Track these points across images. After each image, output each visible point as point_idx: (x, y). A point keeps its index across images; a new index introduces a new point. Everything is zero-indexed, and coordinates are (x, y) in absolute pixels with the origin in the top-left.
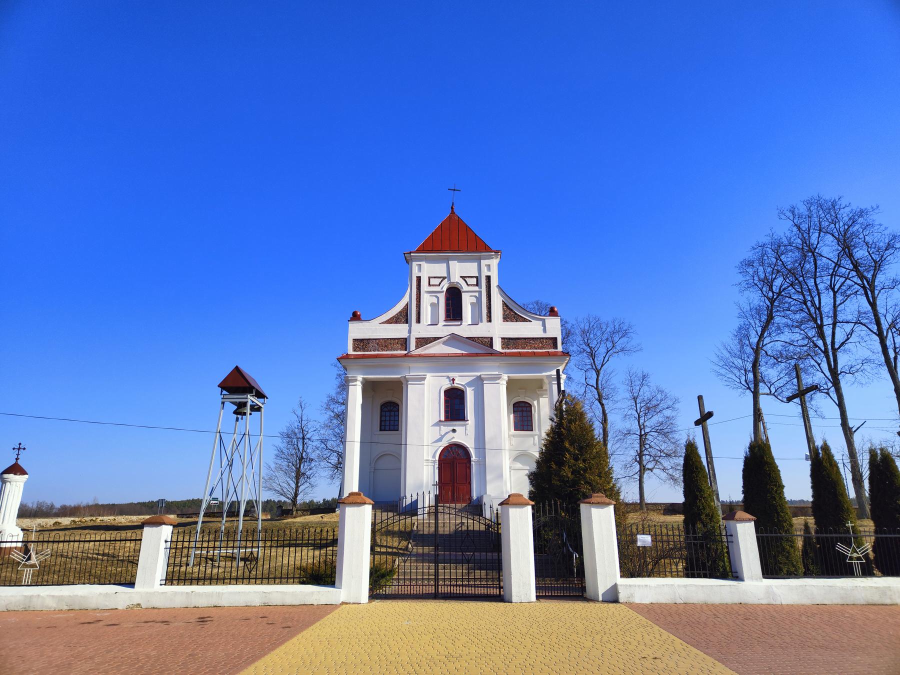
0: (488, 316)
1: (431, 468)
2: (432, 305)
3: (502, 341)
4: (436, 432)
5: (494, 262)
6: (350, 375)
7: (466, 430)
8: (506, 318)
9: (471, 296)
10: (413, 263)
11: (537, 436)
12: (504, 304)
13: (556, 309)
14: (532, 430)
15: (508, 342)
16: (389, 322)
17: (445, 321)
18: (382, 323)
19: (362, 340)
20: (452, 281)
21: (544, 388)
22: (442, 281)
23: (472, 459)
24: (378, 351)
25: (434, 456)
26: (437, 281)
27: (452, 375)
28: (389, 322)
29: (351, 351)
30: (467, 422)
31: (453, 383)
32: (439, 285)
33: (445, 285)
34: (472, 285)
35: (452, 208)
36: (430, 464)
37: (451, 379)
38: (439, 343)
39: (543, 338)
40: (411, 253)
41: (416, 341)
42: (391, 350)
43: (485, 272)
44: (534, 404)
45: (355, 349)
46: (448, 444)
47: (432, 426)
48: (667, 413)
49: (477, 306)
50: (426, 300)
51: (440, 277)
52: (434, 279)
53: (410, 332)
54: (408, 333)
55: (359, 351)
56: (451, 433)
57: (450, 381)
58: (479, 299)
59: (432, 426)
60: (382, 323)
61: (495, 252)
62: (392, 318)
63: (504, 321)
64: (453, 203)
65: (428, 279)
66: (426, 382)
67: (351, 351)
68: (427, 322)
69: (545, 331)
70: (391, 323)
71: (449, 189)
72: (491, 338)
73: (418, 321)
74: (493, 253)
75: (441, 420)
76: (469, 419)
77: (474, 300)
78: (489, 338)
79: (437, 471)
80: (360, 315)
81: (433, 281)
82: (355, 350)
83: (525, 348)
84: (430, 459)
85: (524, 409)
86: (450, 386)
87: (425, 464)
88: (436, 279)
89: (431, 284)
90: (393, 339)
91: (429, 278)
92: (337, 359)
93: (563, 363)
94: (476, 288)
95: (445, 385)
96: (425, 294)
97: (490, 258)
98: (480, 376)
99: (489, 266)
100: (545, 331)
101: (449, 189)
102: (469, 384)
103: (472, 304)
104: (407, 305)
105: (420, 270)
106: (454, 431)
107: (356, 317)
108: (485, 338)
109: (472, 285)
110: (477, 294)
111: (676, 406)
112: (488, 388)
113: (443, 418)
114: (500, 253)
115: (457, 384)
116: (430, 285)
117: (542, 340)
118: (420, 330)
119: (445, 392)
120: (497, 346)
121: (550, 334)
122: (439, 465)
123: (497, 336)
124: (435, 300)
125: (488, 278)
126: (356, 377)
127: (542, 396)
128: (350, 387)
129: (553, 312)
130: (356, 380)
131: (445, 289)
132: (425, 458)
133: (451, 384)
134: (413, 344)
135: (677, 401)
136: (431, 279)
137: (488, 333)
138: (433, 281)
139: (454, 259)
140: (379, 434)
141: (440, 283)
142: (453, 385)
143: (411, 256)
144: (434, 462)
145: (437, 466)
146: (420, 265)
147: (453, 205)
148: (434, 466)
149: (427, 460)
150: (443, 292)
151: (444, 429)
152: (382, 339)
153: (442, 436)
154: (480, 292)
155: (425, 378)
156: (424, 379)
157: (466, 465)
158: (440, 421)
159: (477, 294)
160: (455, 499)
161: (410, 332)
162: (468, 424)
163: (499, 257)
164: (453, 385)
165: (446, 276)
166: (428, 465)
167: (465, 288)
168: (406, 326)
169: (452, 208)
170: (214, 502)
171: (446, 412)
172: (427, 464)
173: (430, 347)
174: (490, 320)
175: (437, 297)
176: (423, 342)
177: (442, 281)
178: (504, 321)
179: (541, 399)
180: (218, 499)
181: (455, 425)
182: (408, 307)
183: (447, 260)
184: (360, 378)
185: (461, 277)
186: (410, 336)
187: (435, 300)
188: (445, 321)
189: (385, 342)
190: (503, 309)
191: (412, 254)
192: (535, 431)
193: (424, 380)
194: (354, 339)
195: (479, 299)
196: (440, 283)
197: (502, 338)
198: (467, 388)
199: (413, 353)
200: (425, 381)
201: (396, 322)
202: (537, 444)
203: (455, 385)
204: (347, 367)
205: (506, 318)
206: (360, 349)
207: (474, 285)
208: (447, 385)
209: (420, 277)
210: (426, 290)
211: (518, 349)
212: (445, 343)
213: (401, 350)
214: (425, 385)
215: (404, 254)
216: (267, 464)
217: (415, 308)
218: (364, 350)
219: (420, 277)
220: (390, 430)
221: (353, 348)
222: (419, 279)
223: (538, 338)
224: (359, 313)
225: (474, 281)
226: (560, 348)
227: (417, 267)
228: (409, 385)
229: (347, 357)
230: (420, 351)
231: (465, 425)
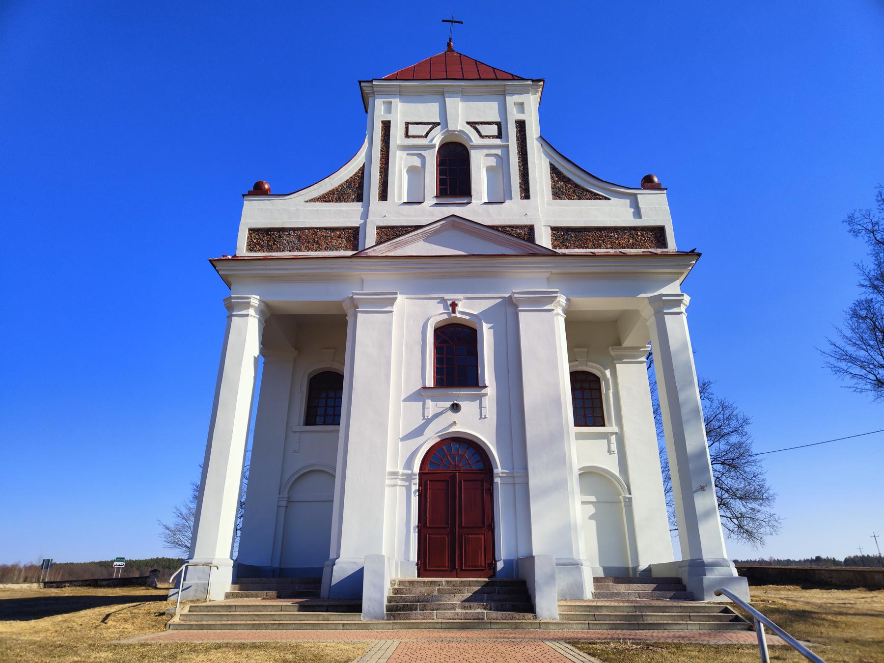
0: (524, 189)
1: (401, 492)
2: (412, 170)
3: (553, 235)
4: (414, 414)
5: (532, 101)
6: (236, 294)
7: (481, 407)
8: (557, 194)
9: (487, 155)
10: (376, 100)
11: (614, 436)
12: (554, 169)
13: (656, 179)
14: (604, 425)
15: (562, 234)
16: (325, 198)
17: (436, 197)
18: (311, 201)
19: (267, 231)
20: (451, 128)
21: (627, 343)
22: (431, 130)
23: (495, 471)
24: (299, 250)
25: (409, 464)
26: (422, 130)
27: (450, 297)
28: (325, 198)
29: (242, 250)
30: (484, 391)
31: (454, 312)
32: (426, 136)
33: (437, 138)
34: (489, 137)
35: (449, 45)
36: (400, 482)
37: (449, 302)
39: (635, 229)
40: (371, 81)
41: (377, 233)
42: (326, 250)
43: (514, 115)
44: (605, 375)
45: (251, 248)
46: (438, 440)
47: (407, 400)
48: (734, 439)
49: (499, 171)
50: (400, 162)
51: (428, 124)
52: (415, 126)
53: (365, 215)
54: (361, 219)
55: (259, 251)
56: (450, 413)
57: (446, 308)
58: (503, 160)
59: (407, 400)
60: (311, 201)
61: (533, 81)
62: (332, 192)
63: (553, 199)
64: (450, 39)
65: (404, 126)
66: (395, 308)
67: (242, 250)
68: (400, 198)
69: (638, 213)
70: (329, 201)
71: (443, 21)
72: (531, 228)
73: (383, 196)
74: (530, 82)
75: (427, 385)
76: (487, 383)
77: (492, 162)
78: (525, 226)
80: (269, 190)
81: (413, 130)
82: (251, 248)
83: (600, 247)
84: (401, 471)
85: (586, 385)
86: (446, 317)
87: (387, 482)
88: (420, 126)
89: (409, 134)
90: (326, 229)
91: (407, 124)
92: (210, 261)
93: (682, 273)
94: (498, 142)
95: (435, 315)
96: (399, 153)
97: (524, 91)
98: (510, 297)
99: (521, 106)
100: (638, 213)
101: (443, 21)
102: (487, 315)
103: (489, 169)
104: (362, 169)
105: (389, 110)
106: (455, 408)
107: (258, 190)
108: (517, 227)
109: (489, 137)
110: (498, 152)
111: (747, 428)
112: (527, 321)
113: (430, 382)
114: (541, 83)
115: (461, 313)
116: (407, 136)
117: (632, 232)
119: (435, 331)
120: (544, 239)
121: (649, 220)
122: (420, 485)
123: (543, 224)
124: (417, 162)
125: (521, 126)
126: (248, 298)
127: (620, 359)
128: (234, 319)
129: (648, 183)
130: (248, 305)
131: (437, 142)
132: (389, 469)
133: (448, 314)
134: (370, 238)
135: (746, 421)
136: (410, 126)
137: (524, 218)
138: (413, 130)
139: (454, 93)
140: (302, 432)
141: (428, 133)
142: (453, 315)
143: (372, 87)
144: (409, 478)
145: (415, 487)
146: (391, 103)
147: (450, 41)
148: (408, 488)
149: (395, 474)
150: (433, 146)
151: (432, 407)
152: (309, 229)
153: (428, 419)
154: (507, 147)
155: (395, 299)
156: (392, 301)
157: (483, 486)
158: (425, 388)
159: (498, 152)
160: (458, 566)
161: (365, 215)
162: (486, 395)
163: (540, 90)
164: (453, 315)
165: (438, 120)
166: (395, 485)
167: (476, 139)
168: (357, 207)
169: (449, 45)
170: (119, 563)
171: (438, 371)
172: (393, 482)
173: (406, 243)
174: (526, 194)
176: (388, 233)
177: (431, 130)
178: (553, 199)
179: (618, 366)
180: (124, 558)
181: (458, 397)
182: (363, 173)
183: (441, 95)
184: (255, 300)
185: (468, 123)
186: (365, 224)
187: (417, 162)
188: (436, 197)
189: (315, 233)
190: (552, 177)
191: (374, 83)
192: (611, 425)
193: (392, 304)
194: (250, 230)
195: (503, 160)
196: (428, 133)
197: (554, 229)
198: (484, 324)
199: (371, 253)
200: (395, 306)
201: (339, 200)
202: (616, 452)
203: (458, 315)
204: (230, 279)
205: (557, 194)
206: (262, 247)
207: (493, 137)
208: (437, 314)
209: (389, 122)
210: (399, 142)
211: (586, 248)
213: (346, 249)
214: (395, 317)
215: (360, 82)
216: (178, 510)
217: (378, 174)
218: (270, 249)
219: (389, 122)
220: (324, 424)
221: (248, 245)
222: (387, 125)
224: (267, 186)
225: (494, 130)
226: (672, 246)
228: (359, 315)
229: (235, 259)
230: (384, 250)
231: (480, 397)
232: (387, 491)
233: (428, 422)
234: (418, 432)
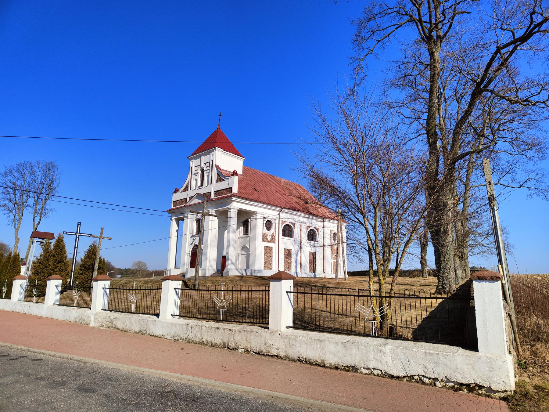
15: (217, 192)
18: (181, 192)
38: (194, 198)
39: (228, 188)
62: (184, 189)
79: (190, 258)
118: (191, 193)
130: (172, 220)
132: (187, 252)
173: (192, 201)
175: (197, 176)
176: (191, 198)
184: (173, 218)
203: (198, 217)
212: (197, 198)
222: (192, 168)
223: (226, 189)
227: (192, 163)
232: (186, 256)
233: (193, 242)
234: (192, 244)
